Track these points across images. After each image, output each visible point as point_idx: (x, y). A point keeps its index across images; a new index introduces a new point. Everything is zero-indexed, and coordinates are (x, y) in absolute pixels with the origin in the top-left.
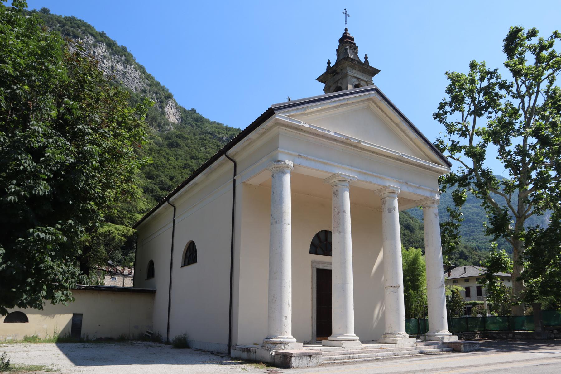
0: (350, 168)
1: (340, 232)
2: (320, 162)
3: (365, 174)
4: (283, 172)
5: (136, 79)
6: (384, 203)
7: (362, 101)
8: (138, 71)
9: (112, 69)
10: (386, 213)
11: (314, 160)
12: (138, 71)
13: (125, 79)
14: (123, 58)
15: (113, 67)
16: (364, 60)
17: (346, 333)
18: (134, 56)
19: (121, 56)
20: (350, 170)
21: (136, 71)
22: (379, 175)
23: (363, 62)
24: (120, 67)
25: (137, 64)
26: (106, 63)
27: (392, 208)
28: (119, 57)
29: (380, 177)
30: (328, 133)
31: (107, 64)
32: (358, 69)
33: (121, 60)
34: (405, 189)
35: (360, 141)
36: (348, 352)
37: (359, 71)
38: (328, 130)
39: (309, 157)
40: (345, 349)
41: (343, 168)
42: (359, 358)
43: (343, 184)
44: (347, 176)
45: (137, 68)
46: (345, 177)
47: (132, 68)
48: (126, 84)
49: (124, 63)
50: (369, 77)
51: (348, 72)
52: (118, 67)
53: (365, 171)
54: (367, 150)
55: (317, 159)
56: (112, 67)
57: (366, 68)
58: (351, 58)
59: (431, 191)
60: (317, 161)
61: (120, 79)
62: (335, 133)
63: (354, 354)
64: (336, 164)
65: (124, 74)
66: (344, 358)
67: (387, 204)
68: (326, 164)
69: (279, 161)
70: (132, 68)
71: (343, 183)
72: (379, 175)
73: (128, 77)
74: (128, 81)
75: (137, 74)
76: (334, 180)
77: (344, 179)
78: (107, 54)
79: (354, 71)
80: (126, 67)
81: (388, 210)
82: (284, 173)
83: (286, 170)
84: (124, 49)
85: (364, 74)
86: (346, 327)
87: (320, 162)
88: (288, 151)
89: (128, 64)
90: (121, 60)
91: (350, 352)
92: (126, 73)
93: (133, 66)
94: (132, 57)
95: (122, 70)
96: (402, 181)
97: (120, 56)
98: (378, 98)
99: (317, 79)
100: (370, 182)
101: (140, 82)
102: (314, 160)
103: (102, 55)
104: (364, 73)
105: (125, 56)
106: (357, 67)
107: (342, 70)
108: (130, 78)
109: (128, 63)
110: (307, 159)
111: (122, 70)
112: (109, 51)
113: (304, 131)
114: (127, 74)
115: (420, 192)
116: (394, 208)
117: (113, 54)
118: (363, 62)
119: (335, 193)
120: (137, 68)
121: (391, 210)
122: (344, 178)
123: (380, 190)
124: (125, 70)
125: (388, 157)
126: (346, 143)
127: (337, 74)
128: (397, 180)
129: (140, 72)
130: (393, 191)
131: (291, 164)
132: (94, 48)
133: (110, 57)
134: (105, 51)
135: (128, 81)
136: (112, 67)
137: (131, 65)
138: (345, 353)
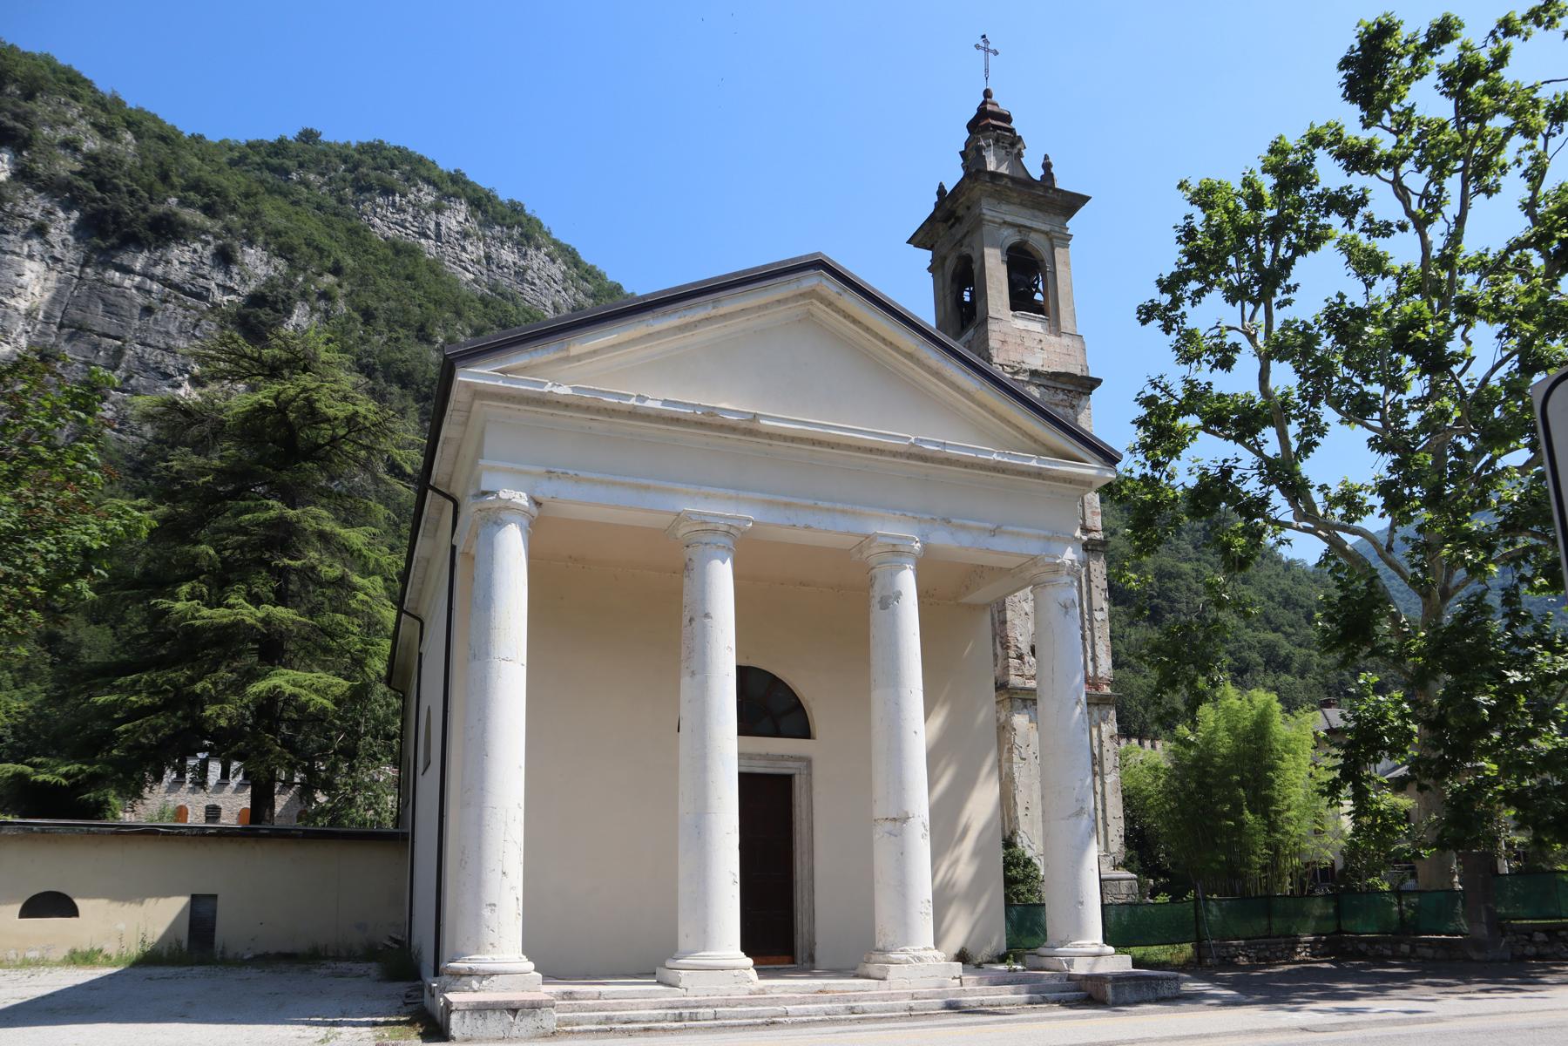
0: (732, 492)
1: (693, 673)
2: (622, 484)
3: (787, 505)
4: (495, 523)
6: (871, 582)
7: (779, 301)
8: (559, 261)
9: (488, 264)
10: (876, 613)
11: (602, 482)
12: (559, 261)
14: (516, 232)
17: (704, 950)
18: (546, 223)
19: (510, 227)
20: (730, 498)
22: (839, 506)
24: (508, 255)
25: (555, 243)
26: (470, 248)
27: (890, 597)
29: (844, 512)
30: (638, 404)
31: (475, 250)
33: (510, 238)
34: (942, 539)
35: (755, 415)
38: (639, 396)
39: (581, 474)
40: (689, 993)
41: (707, 497)
43: (705, 540)
44: (717, 516)
45: (556, 254)
46: (707, 519)
47: (541, 255)
49: (518, 244)
52: (504, 257)
53: (785, 499)
54: (793, 439)
55: (611, 478)
56: (488, 257)
59: (1048, 539)
60: (614, 484)
61: (510, 286)
62: (665, 402)
64: (678, 486)
67: (877, 587)
68: (647, 488)
69: (485, 493)
70: (541, 255)
71: (707, 538)
72: (839, 506)
75: (556, 270)
76: (682, 531)
77: (707, 528)
78: (472, 226)
80: (526, 254)
81: (880, 602)
82: (500, 524)
83: (504, 515)
84: (516, 208)
86: (705, 932)
87: (622, 484)
88: (510, 465)
89: (530, 247)
90: (510, 238)
92: (525, 271)
93: (544, 250)
94: (541, 226)
95: (515, 263)
96: (927, 517)
98: (830, 287)
99: (909, 242)
100: (807, 527)
101: (565, 290)
102: (602, 482)
105: (520, 224)
108: (537, 281)
110: (577, 480)
111: (515, 263)
112: (475, 217)
113: (567, 406)
114: (529, 272)
115: (1000, 544)
116: (898, 596)
117: (486, 224)
119: (687, 567)
120: (556, 254)
121: (890, 600)
122: (706, 523)
123: (860, 547)
124: (522, 263)
125: (871, 451)
126: (710, 423)
128: (910, 514)
129: (565, 263)
130: (891, 548)
131: (521, 499)
134: (467, 220)
136: (488, 257)
138: (676, 1004)
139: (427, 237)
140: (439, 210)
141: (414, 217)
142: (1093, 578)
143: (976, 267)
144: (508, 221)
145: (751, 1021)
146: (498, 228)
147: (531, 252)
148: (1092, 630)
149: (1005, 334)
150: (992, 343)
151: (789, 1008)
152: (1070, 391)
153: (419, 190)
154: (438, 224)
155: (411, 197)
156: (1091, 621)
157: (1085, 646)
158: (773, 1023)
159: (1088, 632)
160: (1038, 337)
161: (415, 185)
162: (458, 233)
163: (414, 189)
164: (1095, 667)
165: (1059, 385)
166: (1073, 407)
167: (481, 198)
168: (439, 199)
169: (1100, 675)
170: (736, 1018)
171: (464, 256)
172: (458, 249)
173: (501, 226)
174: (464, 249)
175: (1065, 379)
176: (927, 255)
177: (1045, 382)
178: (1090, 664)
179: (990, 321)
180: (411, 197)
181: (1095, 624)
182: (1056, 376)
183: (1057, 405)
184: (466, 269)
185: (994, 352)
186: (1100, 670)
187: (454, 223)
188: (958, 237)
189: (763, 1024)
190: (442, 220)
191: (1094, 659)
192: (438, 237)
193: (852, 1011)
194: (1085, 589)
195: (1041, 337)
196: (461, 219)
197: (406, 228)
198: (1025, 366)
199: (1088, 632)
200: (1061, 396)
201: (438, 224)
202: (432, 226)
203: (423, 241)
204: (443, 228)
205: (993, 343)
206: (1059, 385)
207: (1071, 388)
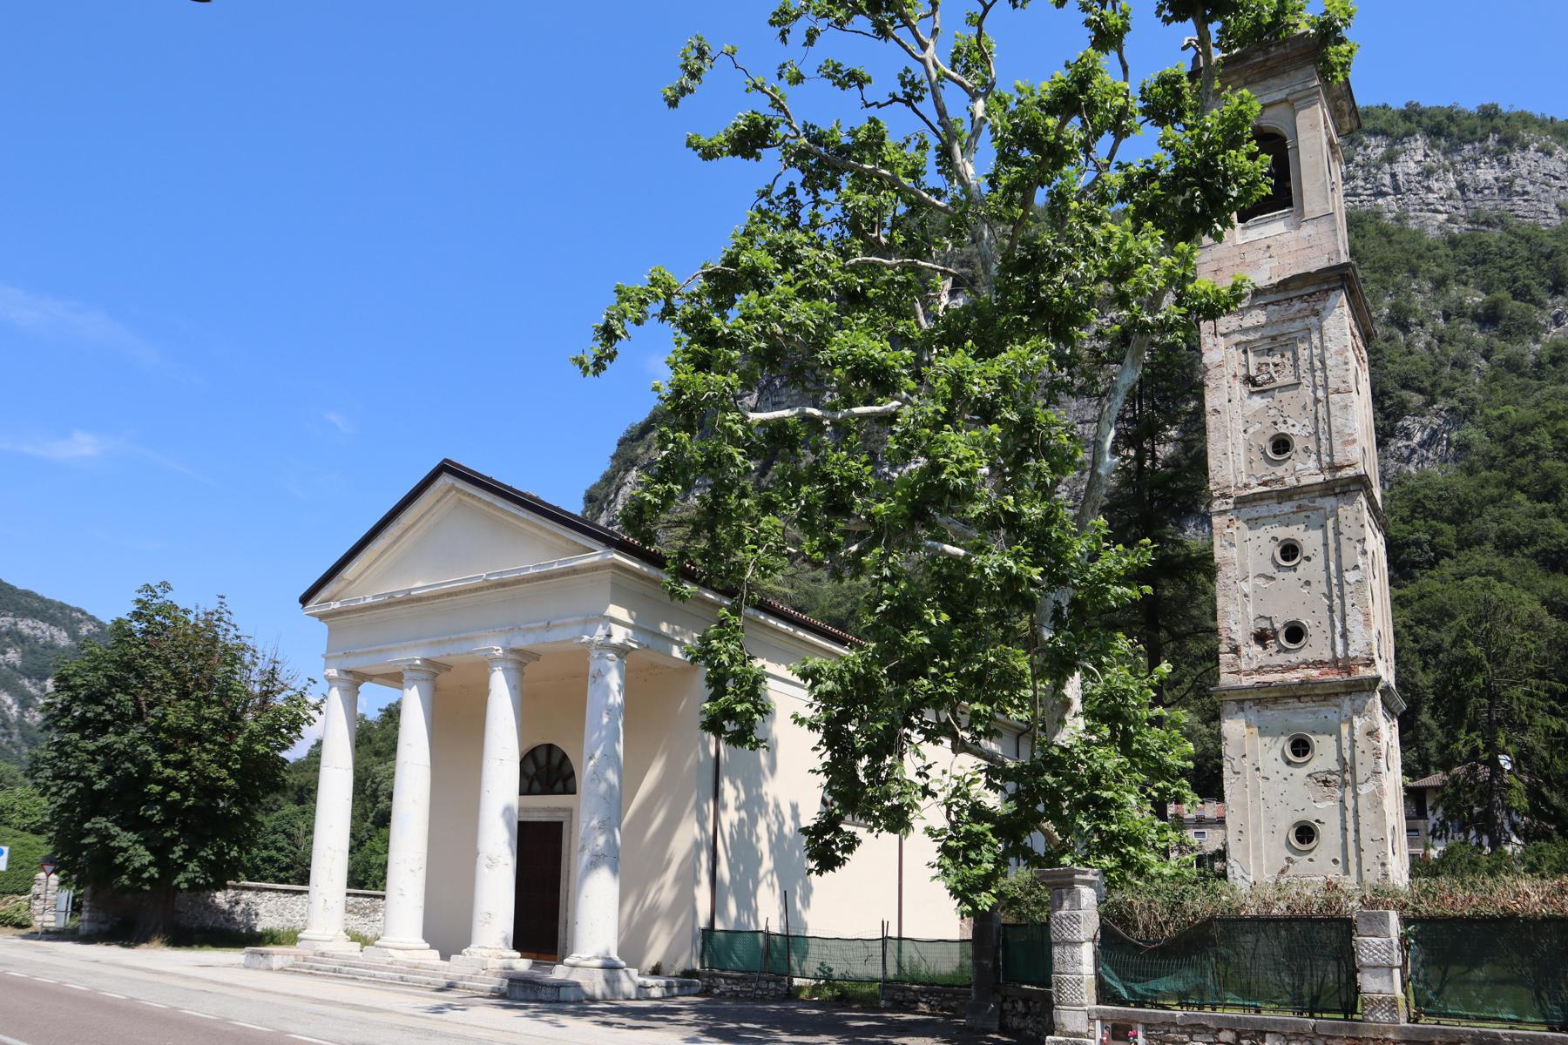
5: (1556, 178)
9: (1463, 193)
13: (1515, 199)
14: (1491, 142)
15: (1464, 185)
21: (1549, 154)
24: (1487, 173)
26: (1435, 185)
28: (1477, 144)
31: (1444, 184)
33: (1485, 152)
48: (1521, 213)
49: (1497, 154)
52: (1482, 177)
65: (1506, 189)
73: (1524, 186)
74: (1525, 201)
78: (1437, 155)
80: (1509, 162)
84: (1489, 114)
89: (1512, 151)
95: (1496, 179)
97: (1481, 141)
103: (1419, 169)
105: (1495, 130)
109: (1509, 147)
111: (1496, 179)
112: (1438, 147)
132: (1390, 164)
133: (1447, 162)
134: (1426, 155)
135: (1525, 201)
136: (1462, 187)
137: (1524, 147)
139: (1384, 194)
140: (1391, 158)
141: (1365, 180)
142: (1342, 528)
144: (1480, 132)
146: (1467, 147)
147: (1516, 156)
148: (1342, 597)
152: (1310, 295)
153: (1366, 148)
154: (1393, 176)
155: (1359, 159)
156: (1341, 586)
157: (1332, 621)
159: (1337, 601)
161: (1361, 144)
162: (1418, 174)
163: (1360, 149)
164: (1346, 645)
165: (1292, 294)
166: (1317, 313)
167: (1439, 123)
168: (1390, 146)
169: (1351, 654)
171: (1431, 197)
172: (1422, 193)
173: (1471, 142)
174: (1429, 190)
175: (1299, 283)
177: (1273, 298)
178: (1339, 642)
180: (1359, 159)
181: (1347, 589)
182: (1284, 285)
183: (1292, 320)
184: (1436, 211)
186: (1351, 648)
187: (1412, 165)
190: (1398, 168)
191: (1344, 636)
192: (1397, 189)
194: (1332, 545)
196: (1419, 157)
197: (1360, 195)
199: (1337, 601)
200: (1298, 305)
201: (1393, 176)
202: (1387, 180)
203: (1380, 201)
204: (1401, 178)
206: (1292, 294)
207: (1312, 290)
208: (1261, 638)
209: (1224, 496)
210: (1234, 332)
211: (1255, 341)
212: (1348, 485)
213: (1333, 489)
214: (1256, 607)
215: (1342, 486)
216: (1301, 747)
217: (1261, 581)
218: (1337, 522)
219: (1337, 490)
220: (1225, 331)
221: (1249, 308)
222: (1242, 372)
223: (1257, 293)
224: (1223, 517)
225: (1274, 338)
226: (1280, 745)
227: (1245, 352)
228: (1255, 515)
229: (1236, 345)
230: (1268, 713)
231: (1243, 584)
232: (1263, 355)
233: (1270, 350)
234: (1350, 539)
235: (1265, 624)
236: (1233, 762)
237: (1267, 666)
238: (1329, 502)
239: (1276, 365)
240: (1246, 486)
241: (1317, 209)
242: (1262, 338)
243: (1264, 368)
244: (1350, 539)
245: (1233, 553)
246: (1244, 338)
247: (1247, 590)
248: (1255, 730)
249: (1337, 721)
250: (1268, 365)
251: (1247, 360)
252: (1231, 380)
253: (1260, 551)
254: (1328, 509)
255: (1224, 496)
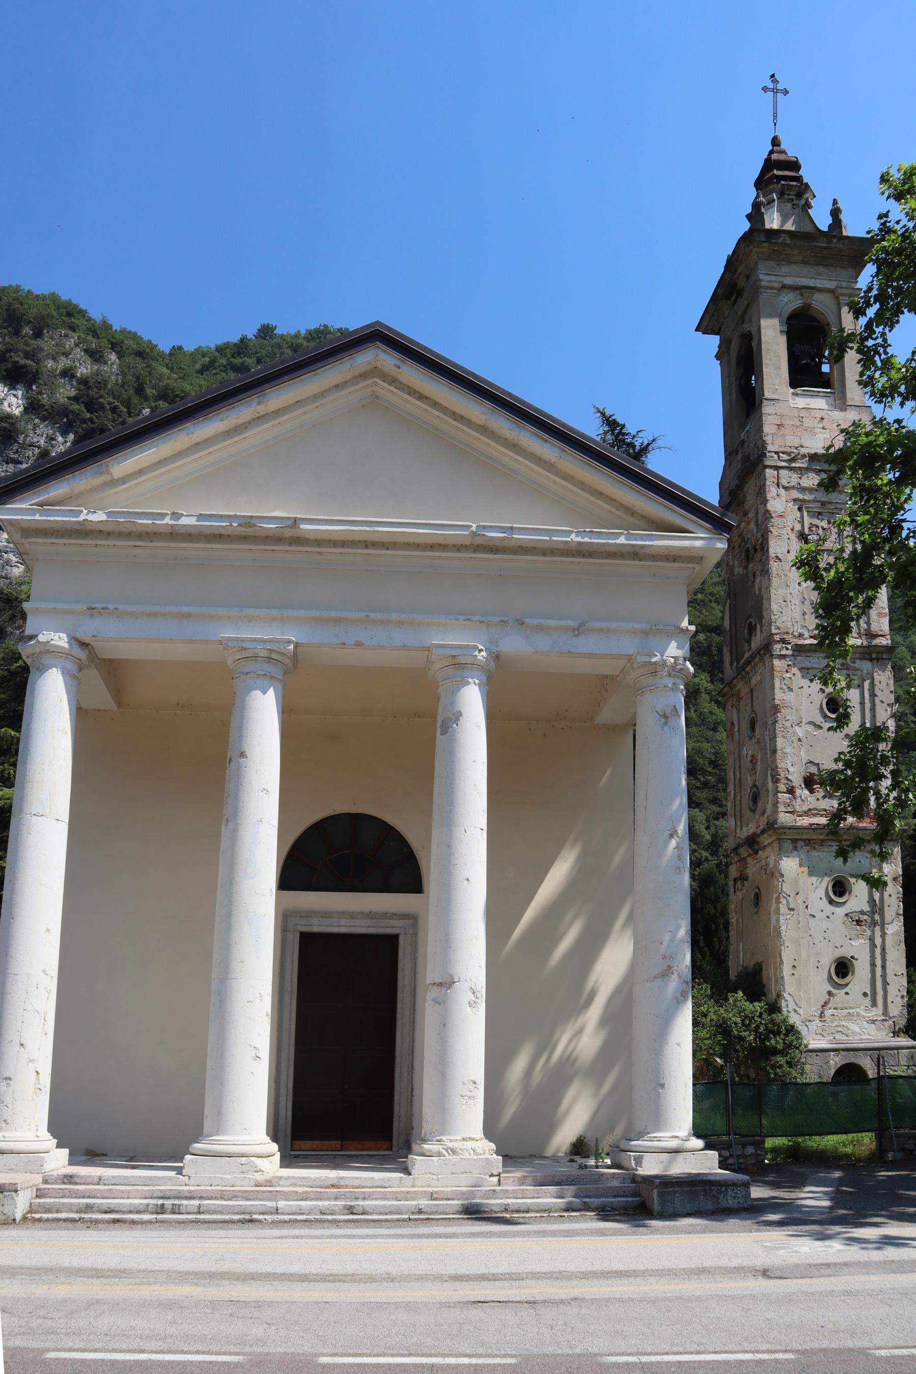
16: (830, 220)
17: (218, 1135)
23: (825, 229)
32: (799, 258)
36: (179, 1192)
37: (804, 262)
40: (192, 1182)
42: (199, 1213)
50: (845, 273)
51: (761, 277)
57: (825, 248)
58: (789, 233)
63: (201, 1198)
66: (141, 1208)
79: (784, 269)
85: (822, 269)
91: (189, 1192)
104: (824, 265)
106: (796, 252)
107: (748, 277)
118: (825, 229)
127: (740, 293)
138: (168, 1194)
143: (754, 344)
145: (227, 1217)
149: (782, 416)
150: (767, 429)
151: (281, 1204)
158: (251, 1221)
160: (819, 414)
170: (221, 1213)
176: (715, 340)
179: (765, 403)
185: (768, 439)
188: (740, 313)
189: (240, 1221)
193: (351, 1210)
195: (822, 414)
198: (803, 451)
205: (768, 428)
208: (809, 782)
209: (783, 641)
210: (793, 488)
211: (809, 501)
212: (882, 653)
213: (870, 654)
214: (807, 751)
215: (878, 653)
216: (840, 888)
217: (811, 728)
218: (872, 684)
219: (874, 656)
220: (787, 485)
221: (807, 469)
222: (798, 527)
223: (814, 457)
224: (783, 661)
225: (823, 504)
226: (824, 885)
227: (800, 509)
228: (809, 665)
229: (795, 500)
230: (815, 854)
231: (797, 728)
232: (813, 517)
233: (820, 514)
234: (882, 702)
235: (814, 770)
236: (790, 899)
237: (815, 809)
238: (866, 666)
239: (824, 529)
240: (801, 636)
241: (856, 398)
242: (815, 501)
243: (814, 529)
244: (882, 702)
245: (789, 697)
246: (801, 496)
247: (801, 735)
248: (806, 869)
249: (868, 866)
250: (817, 527)
251: (802, 517)
252: (790, 532)
253: (810, 699)
254: (865, 672)
255: (783, 641)
